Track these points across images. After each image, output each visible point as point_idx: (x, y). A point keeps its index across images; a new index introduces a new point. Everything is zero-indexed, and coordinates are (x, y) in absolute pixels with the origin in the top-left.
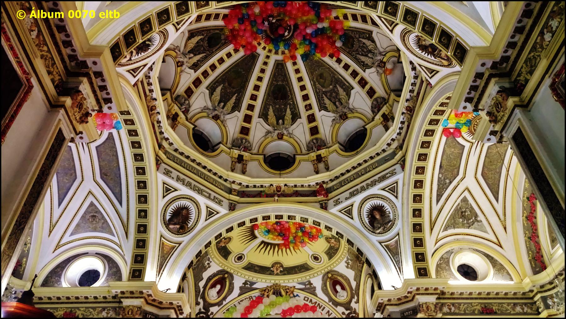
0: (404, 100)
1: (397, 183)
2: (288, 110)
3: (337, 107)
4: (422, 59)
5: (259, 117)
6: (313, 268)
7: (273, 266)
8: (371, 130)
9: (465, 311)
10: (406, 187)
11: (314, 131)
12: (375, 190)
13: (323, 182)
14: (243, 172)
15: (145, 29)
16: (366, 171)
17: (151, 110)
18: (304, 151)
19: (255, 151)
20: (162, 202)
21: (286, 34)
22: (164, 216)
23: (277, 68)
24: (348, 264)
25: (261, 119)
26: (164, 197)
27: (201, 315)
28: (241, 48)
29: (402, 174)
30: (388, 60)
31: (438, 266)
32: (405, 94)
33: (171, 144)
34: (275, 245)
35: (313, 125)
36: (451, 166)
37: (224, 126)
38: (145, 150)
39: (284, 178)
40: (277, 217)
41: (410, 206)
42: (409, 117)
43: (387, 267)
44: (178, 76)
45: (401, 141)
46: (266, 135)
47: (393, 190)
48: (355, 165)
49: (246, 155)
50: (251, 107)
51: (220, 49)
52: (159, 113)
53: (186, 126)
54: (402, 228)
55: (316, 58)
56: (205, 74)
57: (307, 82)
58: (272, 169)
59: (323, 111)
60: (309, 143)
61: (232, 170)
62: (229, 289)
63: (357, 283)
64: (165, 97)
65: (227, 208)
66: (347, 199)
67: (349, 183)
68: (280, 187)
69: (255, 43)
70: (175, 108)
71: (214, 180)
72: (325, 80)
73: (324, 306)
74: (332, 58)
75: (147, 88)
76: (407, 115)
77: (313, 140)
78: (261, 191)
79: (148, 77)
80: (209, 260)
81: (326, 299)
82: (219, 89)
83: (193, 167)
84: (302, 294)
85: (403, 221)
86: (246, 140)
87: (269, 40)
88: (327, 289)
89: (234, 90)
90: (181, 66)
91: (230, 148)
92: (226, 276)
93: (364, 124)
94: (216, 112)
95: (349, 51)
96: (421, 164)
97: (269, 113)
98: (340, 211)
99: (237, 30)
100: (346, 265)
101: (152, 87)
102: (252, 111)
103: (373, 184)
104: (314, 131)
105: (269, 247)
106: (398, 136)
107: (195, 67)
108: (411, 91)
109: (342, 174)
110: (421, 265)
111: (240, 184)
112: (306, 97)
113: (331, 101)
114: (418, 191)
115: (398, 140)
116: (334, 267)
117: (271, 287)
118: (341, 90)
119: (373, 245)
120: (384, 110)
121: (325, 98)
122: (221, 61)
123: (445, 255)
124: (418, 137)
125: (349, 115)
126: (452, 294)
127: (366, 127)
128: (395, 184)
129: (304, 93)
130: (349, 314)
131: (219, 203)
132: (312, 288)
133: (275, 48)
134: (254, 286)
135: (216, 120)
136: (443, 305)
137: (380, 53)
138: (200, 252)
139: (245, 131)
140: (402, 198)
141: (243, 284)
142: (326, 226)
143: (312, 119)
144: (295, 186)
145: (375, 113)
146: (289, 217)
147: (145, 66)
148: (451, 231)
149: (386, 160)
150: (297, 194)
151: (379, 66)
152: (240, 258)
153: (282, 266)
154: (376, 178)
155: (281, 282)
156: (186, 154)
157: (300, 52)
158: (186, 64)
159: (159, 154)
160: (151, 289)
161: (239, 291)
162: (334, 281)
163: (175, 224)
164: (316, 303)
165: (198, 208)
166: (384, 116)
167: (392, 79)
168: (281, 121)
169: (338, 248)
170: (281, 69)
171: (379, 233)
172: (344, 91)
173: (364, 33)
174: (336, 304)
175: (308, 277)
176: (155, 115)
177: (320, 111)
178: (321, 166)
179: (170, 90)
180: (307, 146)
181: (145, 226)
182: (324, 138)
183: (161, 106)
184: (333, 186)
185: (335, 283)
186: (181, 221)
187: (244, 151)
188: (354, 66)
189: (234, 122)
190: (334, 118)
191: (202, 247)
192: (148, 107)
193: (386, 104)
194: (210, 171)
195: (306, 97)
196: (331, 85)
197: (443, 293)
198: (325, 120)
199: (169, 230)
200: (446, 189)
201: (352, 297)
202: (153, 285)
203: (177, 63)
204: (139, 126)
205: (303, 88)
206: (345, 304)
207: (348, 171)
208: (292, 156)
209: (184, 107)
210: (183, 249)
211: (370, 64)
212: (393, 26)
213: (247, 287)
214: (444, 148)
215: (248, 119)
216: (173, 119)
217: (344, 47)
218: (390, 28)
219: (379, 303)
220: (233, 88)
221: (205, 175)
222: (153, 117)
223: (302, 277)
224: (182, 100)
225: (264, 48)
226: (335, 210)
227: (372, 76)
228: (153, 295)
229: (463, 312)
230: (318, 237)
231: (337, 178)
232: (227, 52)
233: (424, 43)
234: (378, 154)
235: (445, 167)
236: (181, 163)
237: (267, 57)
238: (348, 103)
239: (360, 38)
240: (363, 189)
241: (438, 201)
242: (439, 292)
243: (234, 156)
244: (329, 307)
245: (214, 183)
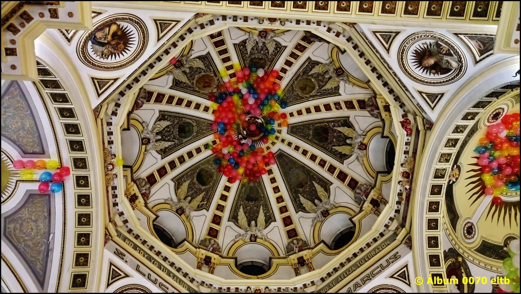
47: (388, 37)
57: (311, 104)
69: (266, 152)
72: (306, 85)
82: (302, 200)
87: (264, 139)
89: (309, 183)
95: (269, 61)
97: (340, 151)
119: (481, 73)
131: (396, 257)
135: (329, 214)
150: (414, 155)
170: (297, 129)
172: (314, 67)
173: (240, 50)
209: (295, 249)
220: (307, 183)
225: (273, 144)
237: (282, 141)
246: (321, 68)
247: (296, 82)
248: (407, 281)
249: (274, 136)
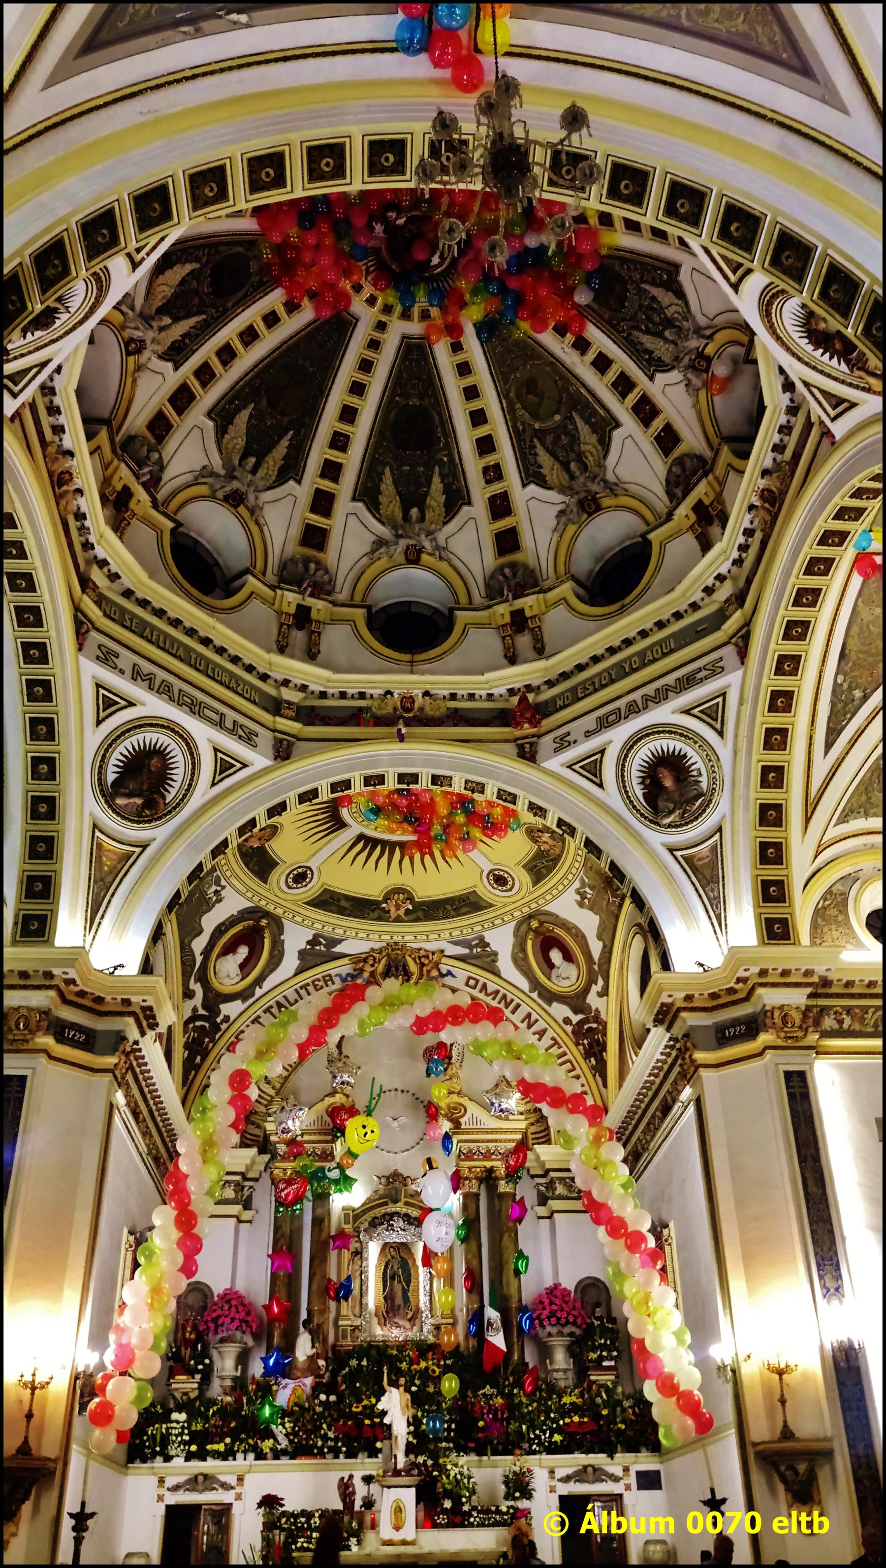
0: (758, 472)
1: (724, 695)
2: (436, 479)
3: (572, 477)
4: (814, 368)
5: (354, 499)
6: (491, 905)
7: (386, 899)
8: (662, 546)
10: (747, 709)
11: (507, 542)
12: (663, 713)
13: (529, 688)
14: (312, 655)
15: (50, 272)
16: (644, 660)
17: (60, 483)
18: (478, 599)
19: (343, 596)
20: (95, 737)
21: (435, 260)
22: (100, 773)
23: (405, 358)
24: (583, 896)
26: (99, 722)
27: (198, 1023)
28: (306, 302)
29: (739, 674)
30: (719, 353)
31: (819, 913)
32: (761, 454)
33: (114, 577)
34: (393, 845)
35: (504, 523)
36: (871, 655)
37: (257, 522)
38: (46, 597)
39: (423, 673)
40: (401, 778)
41: (755, 757)
42: (768, 518)
43: (686, 912)
44: (129, 380)
45: (741, 583)
46: (373, 551)
47: (713, 713)
48: (616, 643)
49: (318, 606)
50: (332, 470)
51: (246, 301)
52: (79, 491)
53: (153, 526)
54: (731, 814)
55: (518, 335)
56: (205, 374)
57: (490, 401)
58: (388, 646)
59: (532, 487)
60: (493, 576)
61: (282, 650)
63: (605, 946)
64: (95, 443)
65: (270, 752)
66: (588, 734)
67: (596, 691)
68: (412, 700)
69: (346, 285)
70: (124, 475)
71: (232, 675)
73: (517, 1001)
74: (563, 335)
75: (46, 421)
76: (762, 512)
77: (500, 569)
78: (361, 709)
79: (48, 390)
80: (218, 883)
81: (524, 984)
82: (242, 418)
83: (174, 640)
84: (462, 972)
85: (733, 795)
86: (318, 563)
88: (526, 958)
89: (286, 420)
90: (139, 351)
91: (273, 588)
92: (264, 922)
93: (644, 528)
94: (236, 484)
96: (791, 648)
97: (383, 487)
98: (570, 767)
99: (296, 248)
100: (578, 898)
101: (62, 420)
102: (335, 480)
103: (661, 696)
104: (507, 542)
105: (379, 849)
106: (735, 569)
107: (176, 354)
108: (778, 448)
109: (580, 668)
110: (775, 910)
111: (303, 688)
112: (486, 445)
114: (778, 720)
115: (735, 579)
116: (548, 902)
117: (380, 951)
118: (584, 429)
119: (652, 855)
120: (701, 490)
122: (249, 336)
123: (839, 887)
124: (787, 574)
125: (606, 502)
126: (849, 984)
127: (651, 536)
128: (720, 699)
129: (483, 431)
130: (581, 1023)
131: (249, 738)
132: (489, 955)
133: (402, 300)
134: (338, 949)
135: (236, 507)
136: (823, 1010)
137: (698, 331)
138: (200, 866)
139: (314, 537)
140: (736, 736)
141: (308, 943)
142: (530, 803)
143: (500, 506)
144: (453, 697)
145: (675, 500)
146: (436, 780)
147: (44, 365)
149: (697, 632)
150: (457, 717)
151: (692, 367)
152: (301, 877)
153: (411, 898)
154: (670, 679)
155: (406, 938)
156: (156, 605)
157: (472, 315)
158: (150, 347)
159: (83, 606)
160: (73, 967)
162: (545, 939)
163: (129, 795)
164: (497, 992)
165: (191, 754)
166: (699, 508)
167: (728, 407)
168: (414, 512)
169: (559, 857)
171: (669, 826)
172: (594, 431)
173: (655, 268)
174: (550, 997)
176: (70, 496)
177: (524, 485)
178: (524, 641)
179: (107, 422)
180: (487, 585)
181: (51, 802)
182: (532, 562)
183: (85, 472)
184: (554, 699)
185: (548, 943)
186: (145, 788)
187: (312, 595)
188: (623, 361)
189: (283, 514)
190: (562, 507)
191: (203, 855)
192: (51, 474)
193: (705, 475)
194: (221, 651)
195: (486, 445)
196: (558, 412)
197: (826, 982)
198: (537, 511)
199: (114, 811)
200: (853, 715)
201: (591, 981)
202: (77, 956)
203: (127, 343)
204: (29, 532)
205: (478, 418)
206: (571, 997)
207: (596, 659)
208: (446, 612)
209: (146, 470)
210: (154, 861)
211: (667, 359)
212: (740, 272)
213: (318, 952)
214: (856, 605)
215: (323, 503)
216: (118, 504)
217: (596, 307)
218: (733, 278)
219: (663, 1004)
221: (209, 662)
222: (63, 502)
223: (463, 926)
224: (138, 450)
225: (371, 301)
226: (555, 763)
227: (669, 391)
228: (79, 982)
229: (870, 1029)
230: (507, 826)
231: (565, 676)
232: (267, 311)
233: (822, 325)
234: (678, 616)
235: (853, 657)
236: (142, 630)
237: (379, 328)
238: (602, 467)
239: (643, 282)
240: (634, 710)
241: (829, 746)
242: (815, 979)
243: (285, 609)
244: (531, 1004)
245: (233, 684)
246: (595, 453)
247: (549, 369)
248: (218, 778)
249: (391, 300)
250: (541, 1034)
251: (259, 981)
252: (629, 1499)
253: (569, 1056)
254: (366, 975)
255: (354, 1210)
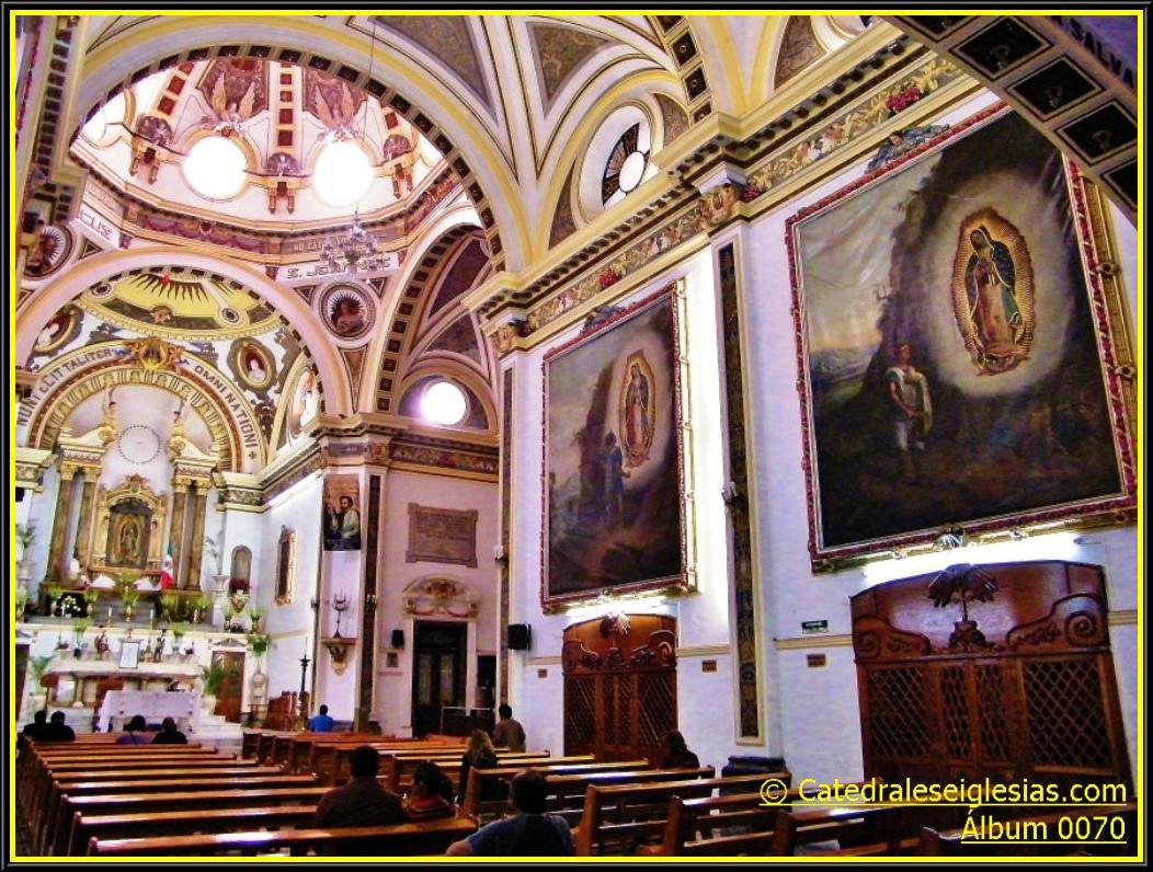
2: (251, 90)
7: (154, 311)
9: (419, 458)
11: (285, 138)
24: (279, 337)
25: (201, 93)
35: (286, 127)
47: (380, 284)
62: (72, 333)
73: (225, 385)
81: (231, 376)
88: (236, 363)
104: (285, 138)
113: (326, 101)
117: (145, 339)
121: (318, 93)
130: (261, 405)
134: (117, 334)
141: (99, 327)
148: (436, 352)
153: (170, 313)
161: (89, 338)
162: (250, 354)
164: (214, 378)
168: (234, 106)
174: (245, 386)
175: (209, 339)
185: (251, 356)
213: (103, 334)
223: (203, 336)
229: (416, 459)
241: (432, 314)
250: (236, 407)
251: (62, 346)
252: (247, 655)
253: (250, 423)
254: (133, 353)
255: (108, 492)
